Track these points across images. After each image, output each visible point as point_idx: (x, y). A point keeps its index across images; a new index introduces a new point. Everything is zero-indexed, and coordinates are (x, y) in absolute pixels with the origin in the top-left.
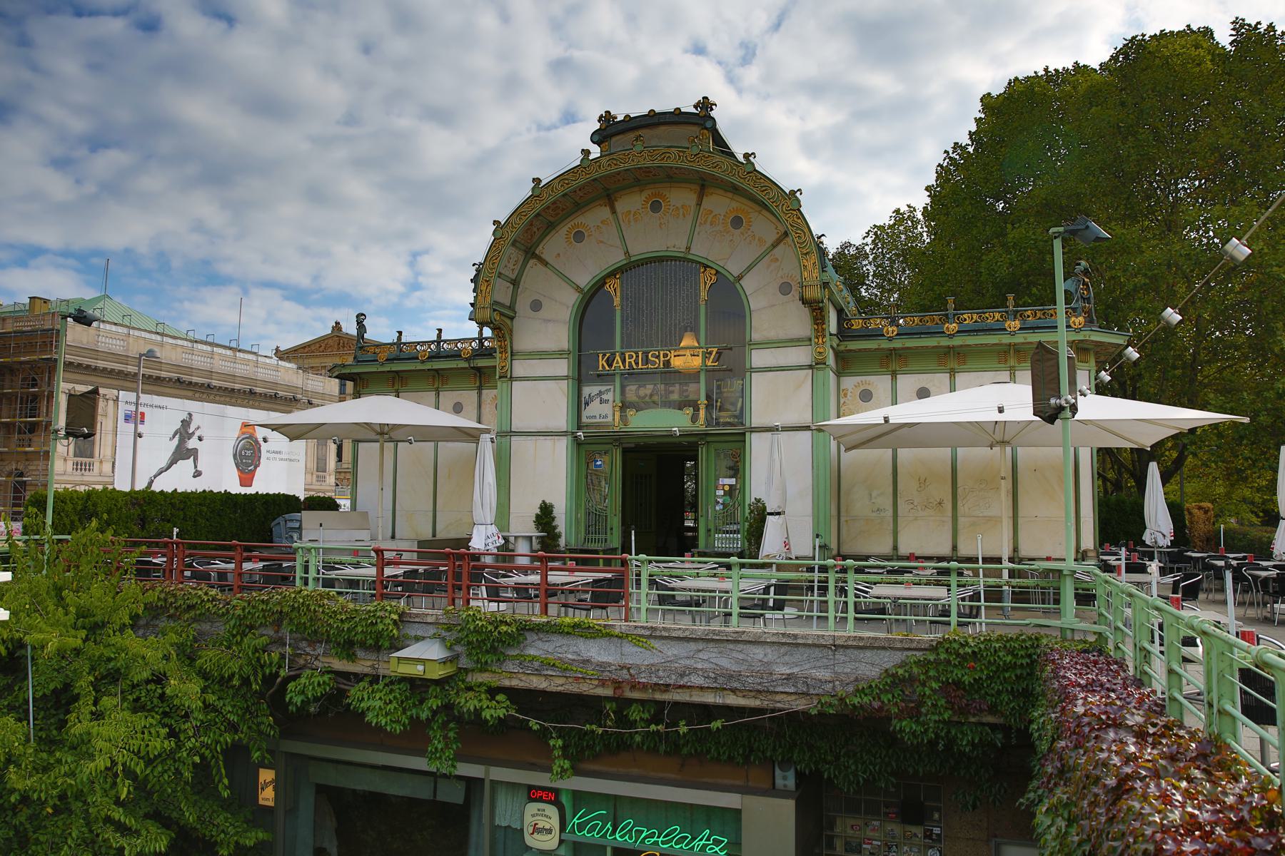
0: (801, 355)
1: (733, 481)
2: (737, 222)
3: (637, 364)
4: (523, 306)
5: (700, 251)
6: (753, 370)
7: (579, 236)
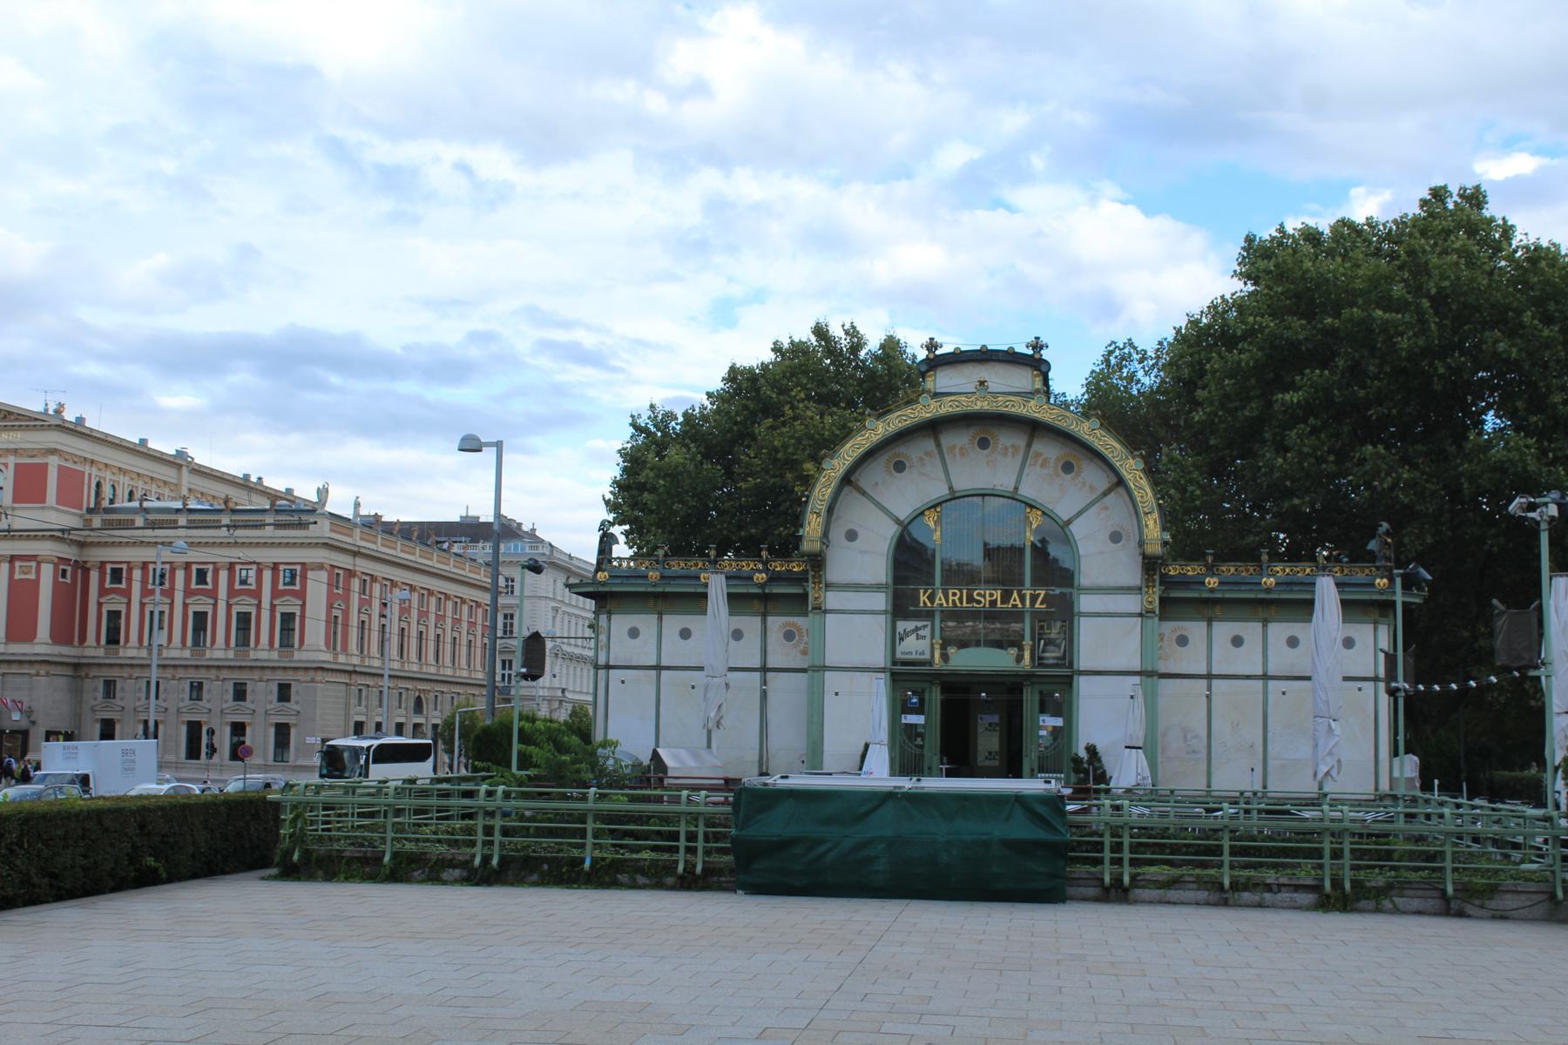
0: (1132, 603)
1: (1059, 722)
2: (1068, 468)
3: (961, 599)
4: (837, 535)
5: (1026, 491)
6: (1081, 614)
7: (900, 467)
